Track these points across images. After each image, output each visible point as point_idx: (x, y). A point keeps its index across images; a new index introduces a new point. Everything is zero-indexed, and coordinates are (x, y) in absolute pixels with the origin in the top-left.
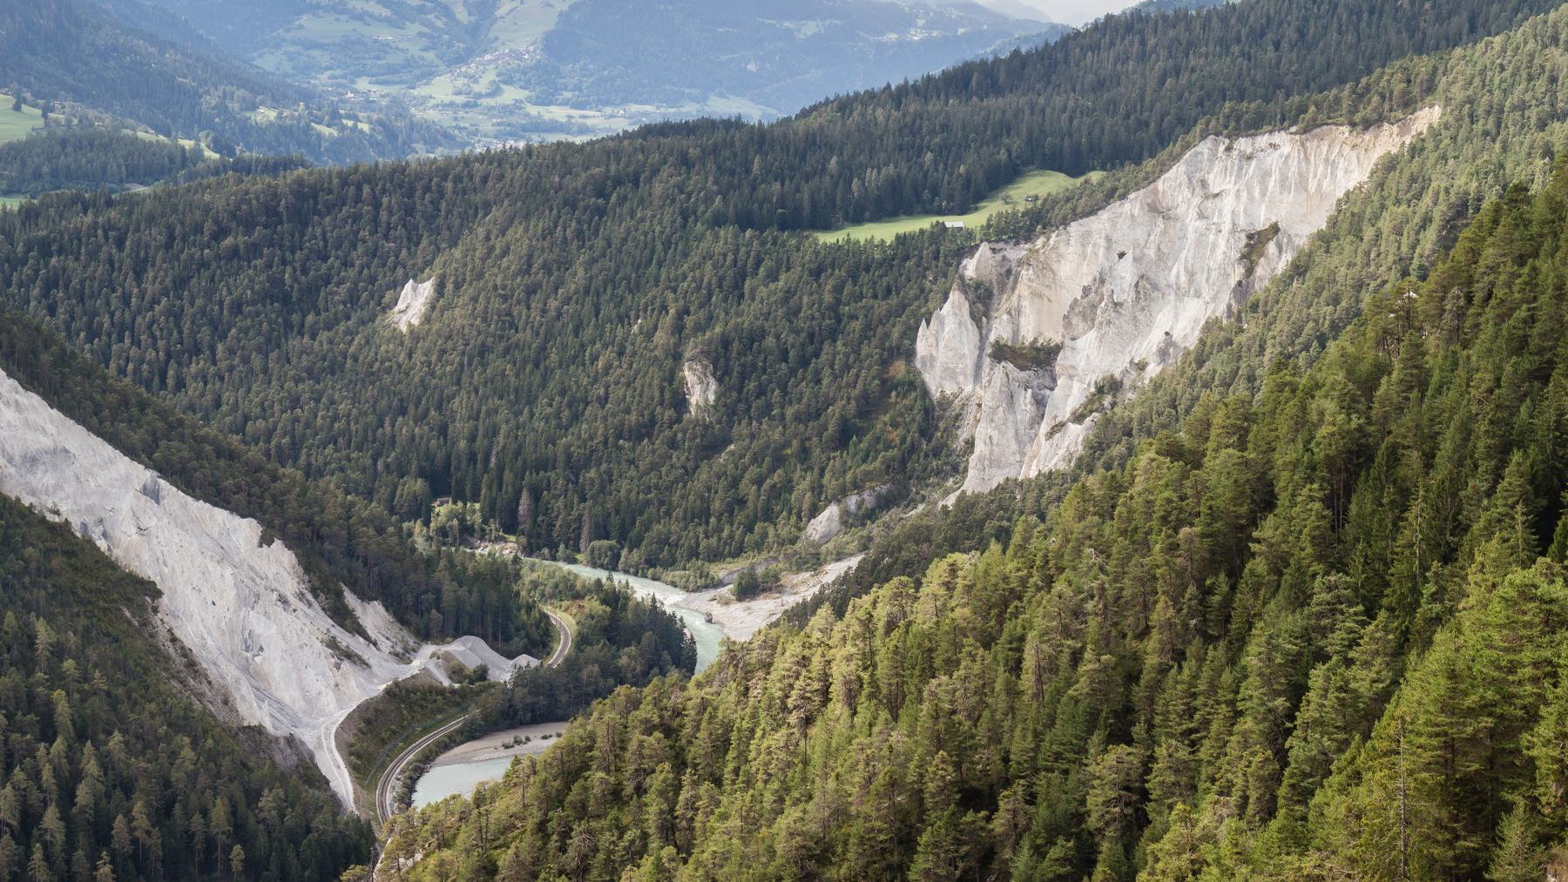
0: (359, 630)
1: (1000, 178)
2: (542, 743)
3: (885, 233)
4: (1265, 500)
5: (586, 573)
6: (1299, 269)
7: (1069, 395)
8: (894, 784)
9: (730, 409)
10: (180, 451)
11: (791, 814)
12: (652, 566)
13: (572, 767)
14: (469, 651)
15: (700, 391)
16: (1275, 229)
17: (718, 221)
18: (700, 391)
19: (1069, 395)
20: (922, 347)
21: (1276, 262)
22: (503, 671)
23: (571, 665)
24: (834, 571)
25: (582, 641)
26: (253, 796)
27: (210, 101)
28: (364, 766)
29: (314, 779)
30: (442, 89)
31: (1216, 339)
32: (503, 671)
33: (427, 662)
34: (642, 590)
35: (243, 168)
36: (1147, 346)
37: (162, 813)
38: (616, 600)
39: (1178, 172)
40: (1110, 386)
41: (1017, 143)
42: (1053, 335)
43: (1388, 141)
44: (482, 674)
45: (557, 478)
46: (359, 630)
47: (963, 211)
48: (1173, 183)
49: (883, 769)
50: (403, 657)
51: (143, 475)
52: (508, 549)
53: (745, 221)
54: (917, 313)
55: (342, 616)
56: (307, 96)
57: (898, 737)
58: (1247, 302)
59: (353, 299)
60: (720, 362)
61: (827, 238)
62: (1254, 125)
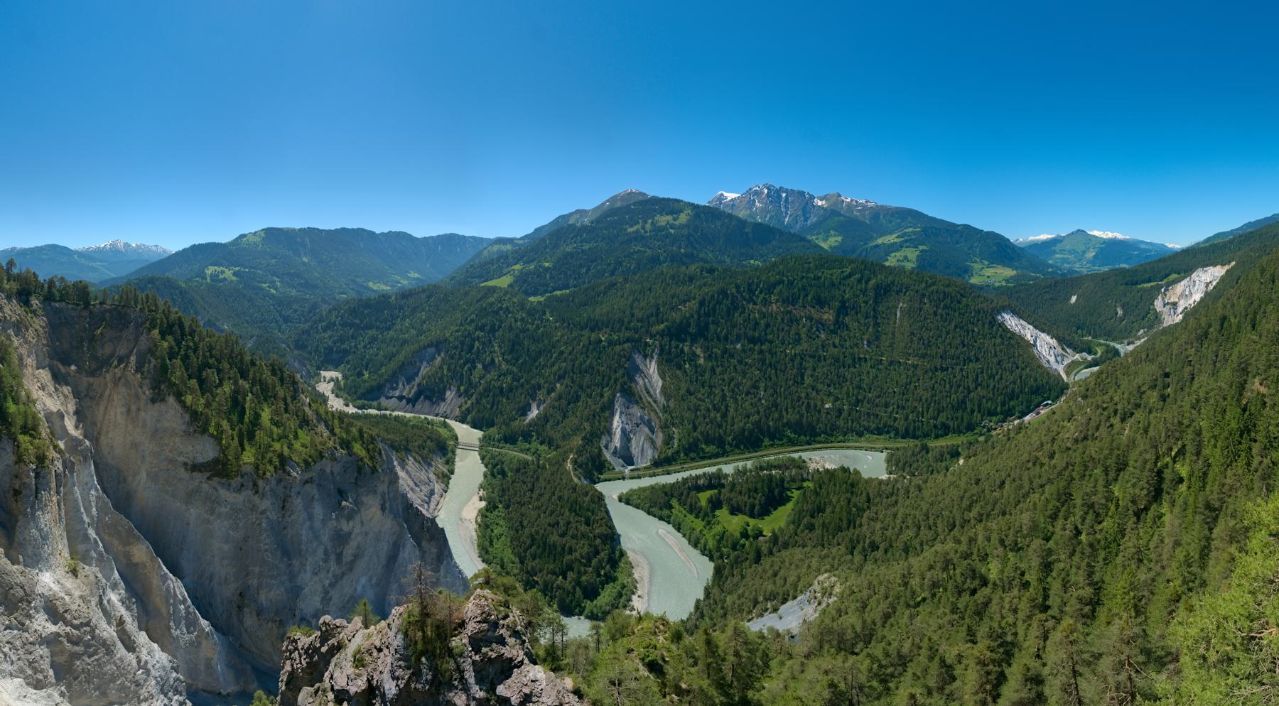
0: (1066, 352)
1: (1167, 276)
2: (1096, 369)
3: (1149, 285)
4: (1210, 326)
5: (1102, 341)
6: (1214, 288)
7: (1180, 310)
8: (1153, 375)
9: (1125, 315)
10: (1036, 323)
11: (1136, 380)
12: (1113, 340)
13: (1101, 372)
14: (1085, 354)
15: (1120, 312)
16: (1211, 282)
17: (1122, 284)
18: (1120, 312)
19: (1180, 310)
20: (1155, 303)
21: (1211, 287)
22: (1090, 358)
23: (1101, 357)
24: (1143, 340)
25: (1102, 353)
26: (1049, 378)
27: (1041, 268)
28: (1068, 374)
29: (1059, 374)
30: (1078, 265)
31: (1202, 300)
32: (1090, 358)
33: (1077, 356)
34: (1112, 344)
35: (1046, 279)
36: (1191, 301)
37: (1036, 380)
38: (1108, 346)
39: (1195, 273)
40: (1186, 308)
41: (1170, 269)
42: (1177, 300)
43: (1227, 267)
44: (1086, 359)
45: (1097, 328)
46: (1066, 352)
47: (1162, 280)
48: (1194, 276)
49: (1151, 372)
50: (1074, 356)
51: (1031, 327)
52: (1090, 338)
53: (1127, 284)
54: (1154, 298)
55: (1063, 349)
56: (1057, 267)
57: (1153, 367)
58: (1206, 294)
59: (1064, 299)
60: (1123, 307)
61: (1139, 286)
62: (1207, 266)
